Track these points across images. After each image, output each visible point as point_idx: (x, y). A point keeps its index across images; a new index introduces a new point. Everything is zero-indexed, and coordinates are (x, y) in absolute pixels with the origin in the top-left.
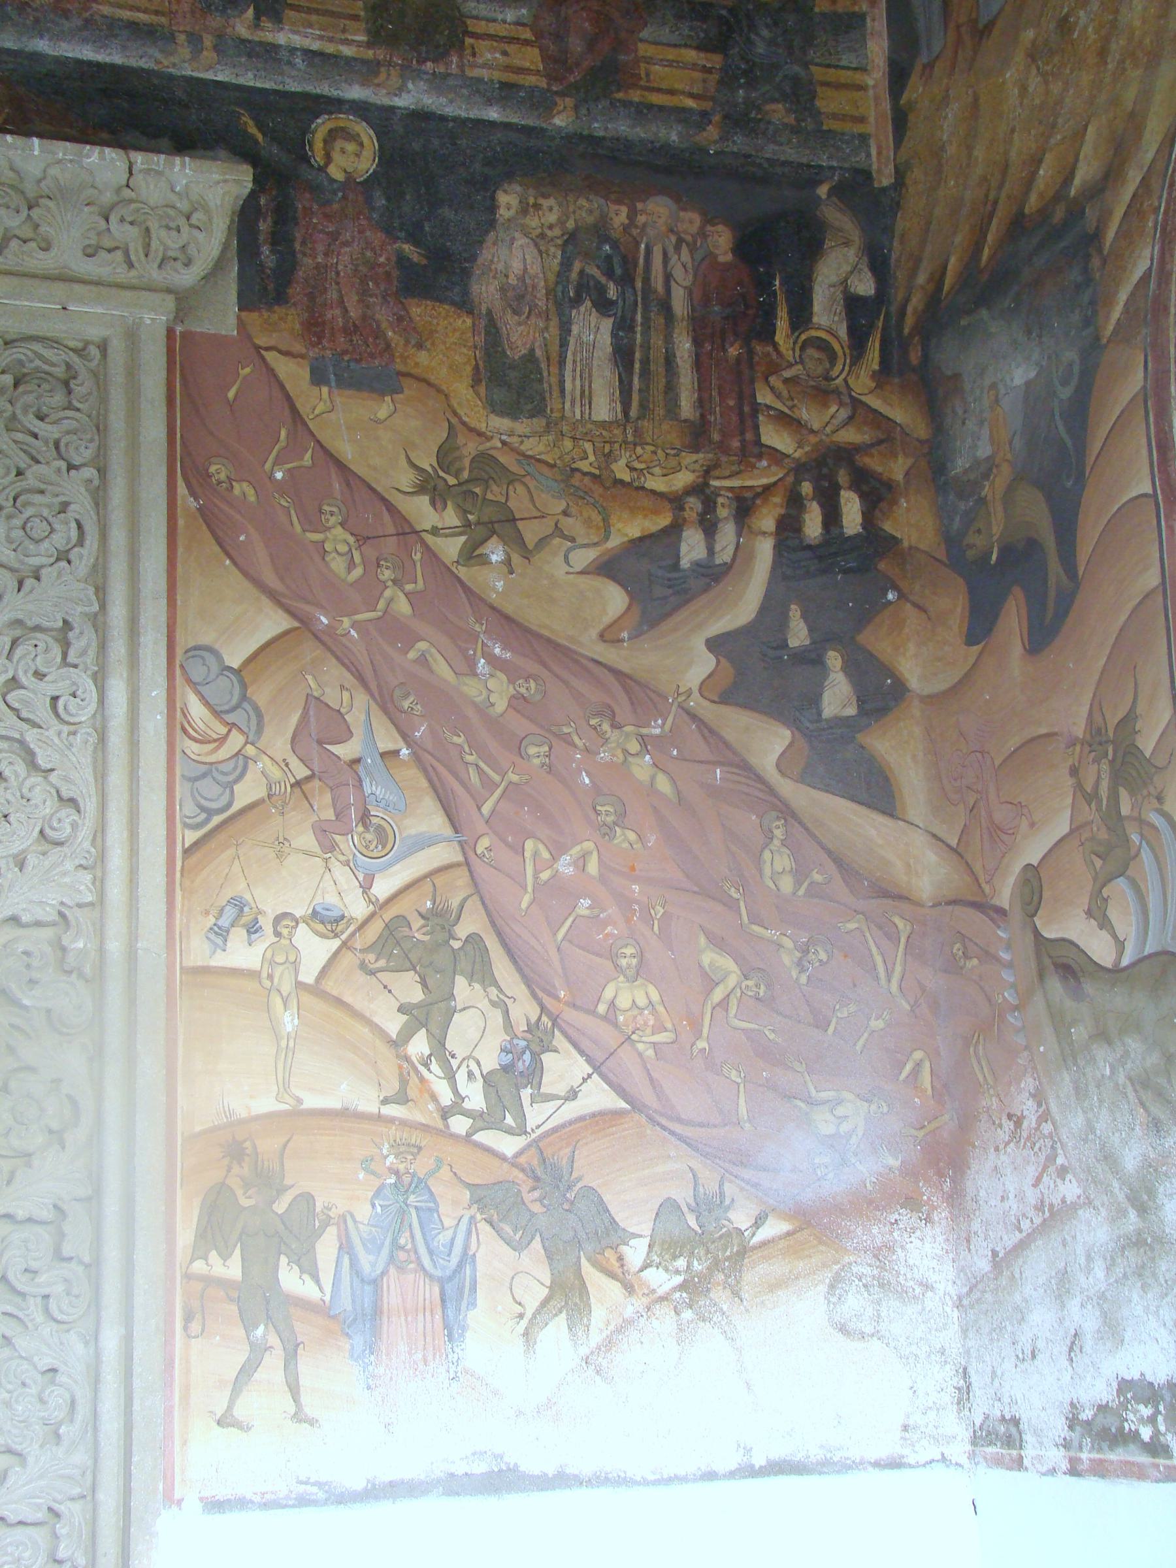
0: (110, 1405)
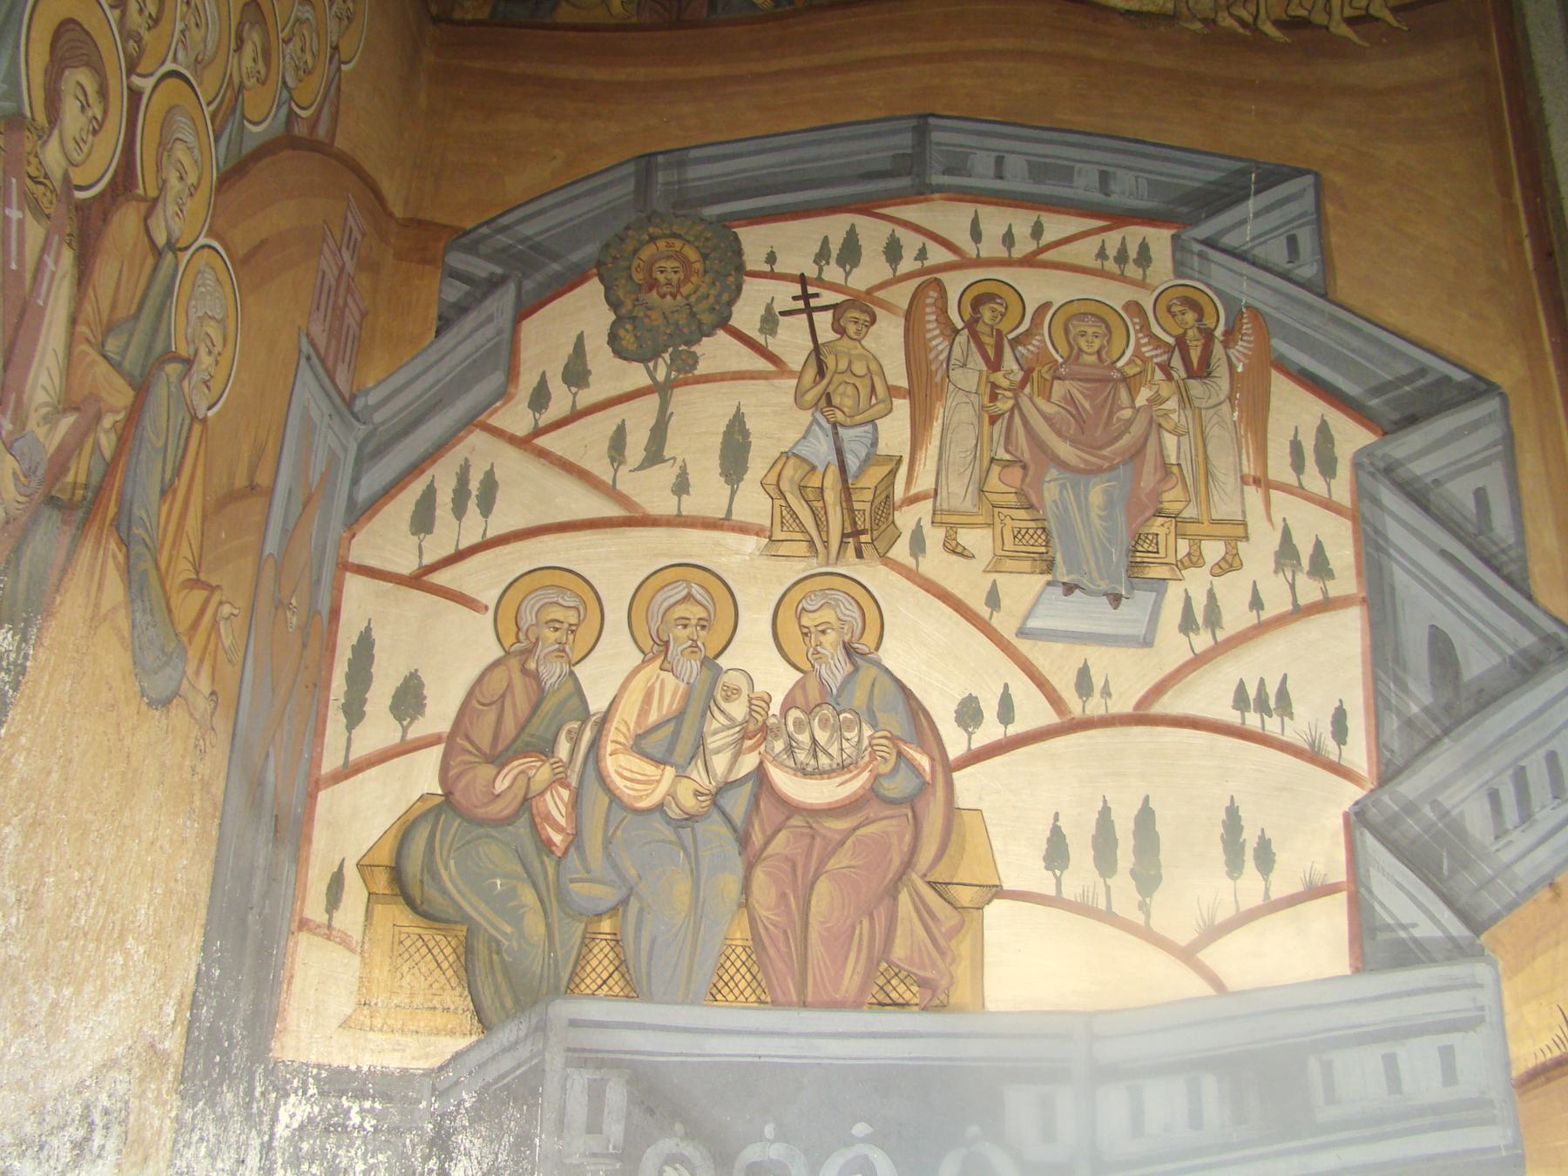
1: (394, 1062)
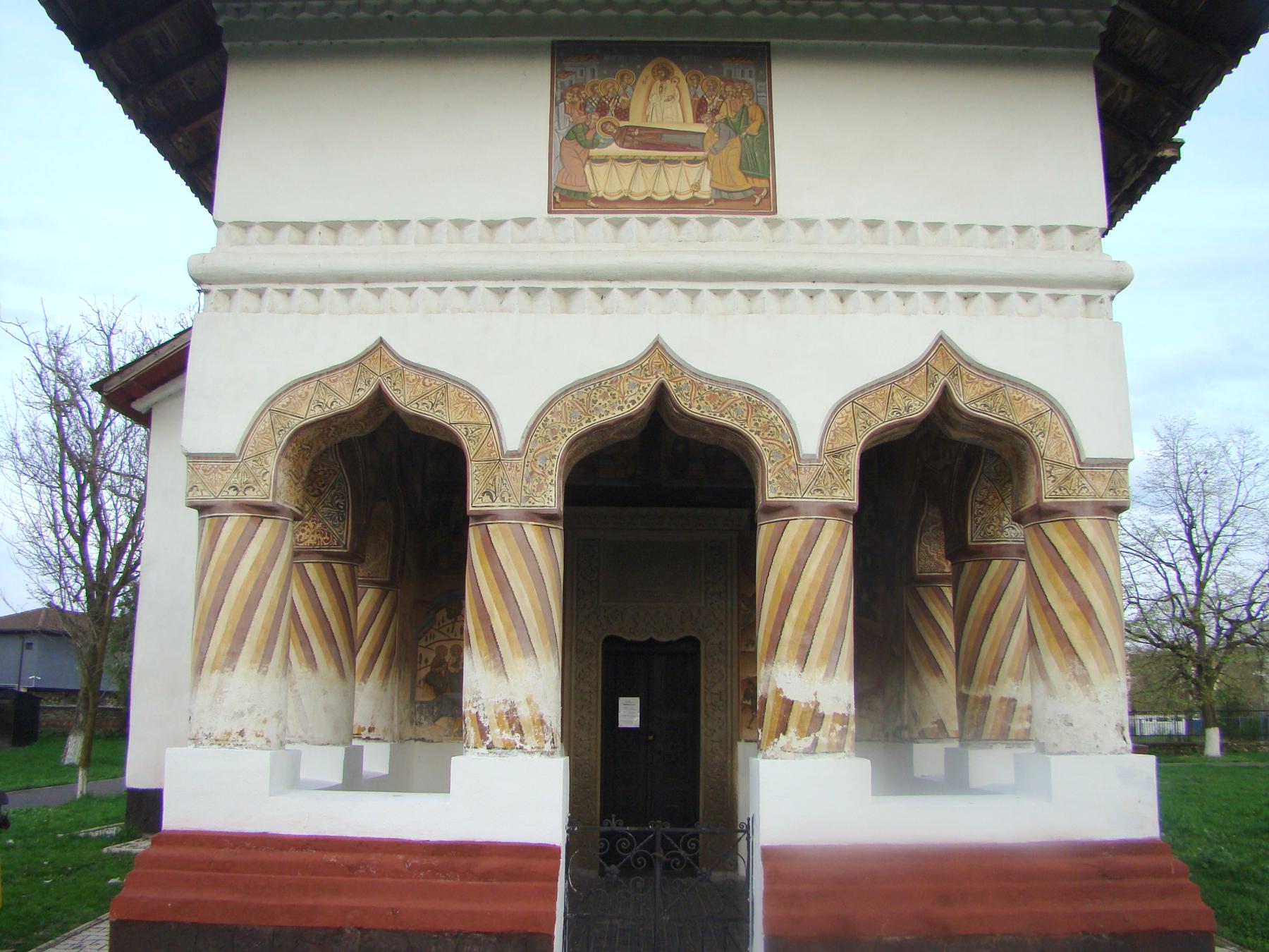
0: (729, 723)
1: (427, 700)
